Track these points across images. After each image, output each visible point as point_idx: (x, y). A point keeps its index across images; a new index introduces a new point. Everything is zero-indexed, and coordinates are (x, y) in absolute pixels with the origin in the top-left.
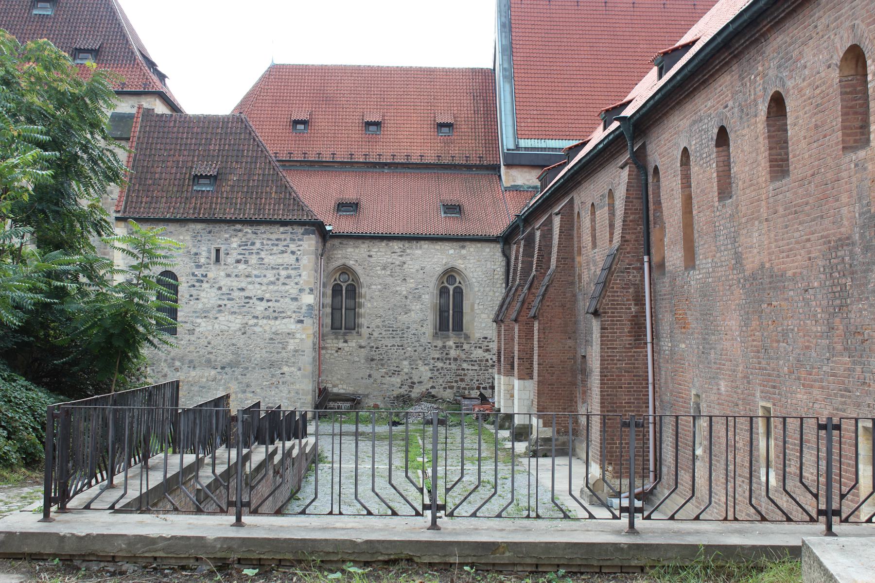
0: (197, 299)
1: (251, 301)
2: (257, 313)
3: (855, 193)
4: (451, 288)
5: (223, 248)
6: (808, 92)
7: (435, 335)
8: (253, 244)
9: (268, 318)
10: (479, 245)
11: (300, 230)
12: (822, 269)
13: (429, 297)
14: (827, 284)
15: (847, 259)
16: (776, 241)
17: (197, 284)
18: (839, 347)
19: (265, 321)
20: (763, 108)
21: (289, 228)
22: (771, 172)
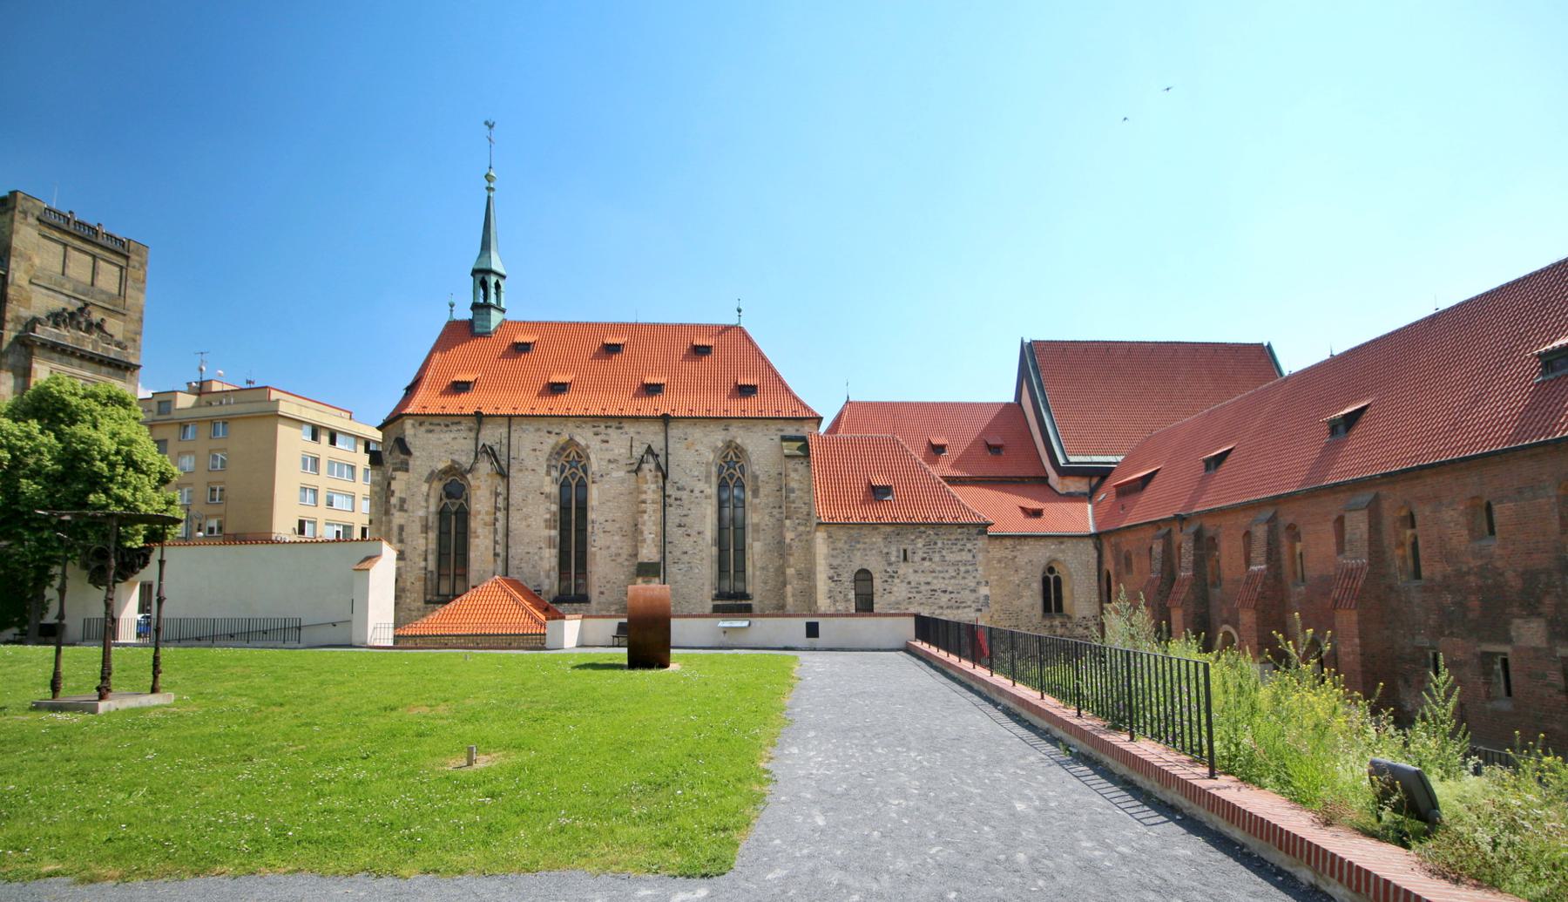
0: (890, 593)
1: (937, 594)
2: (942, 604)
4: (1052, 577)
5: (909, 548)
7: (1044, 617)
8: (935, 543)
9: (951, 607)
10: (1074, 541)
11: (974, 531)
13: (1037, 586)
17: (890, 580)
19: (949, 611)
21: (965, 530)
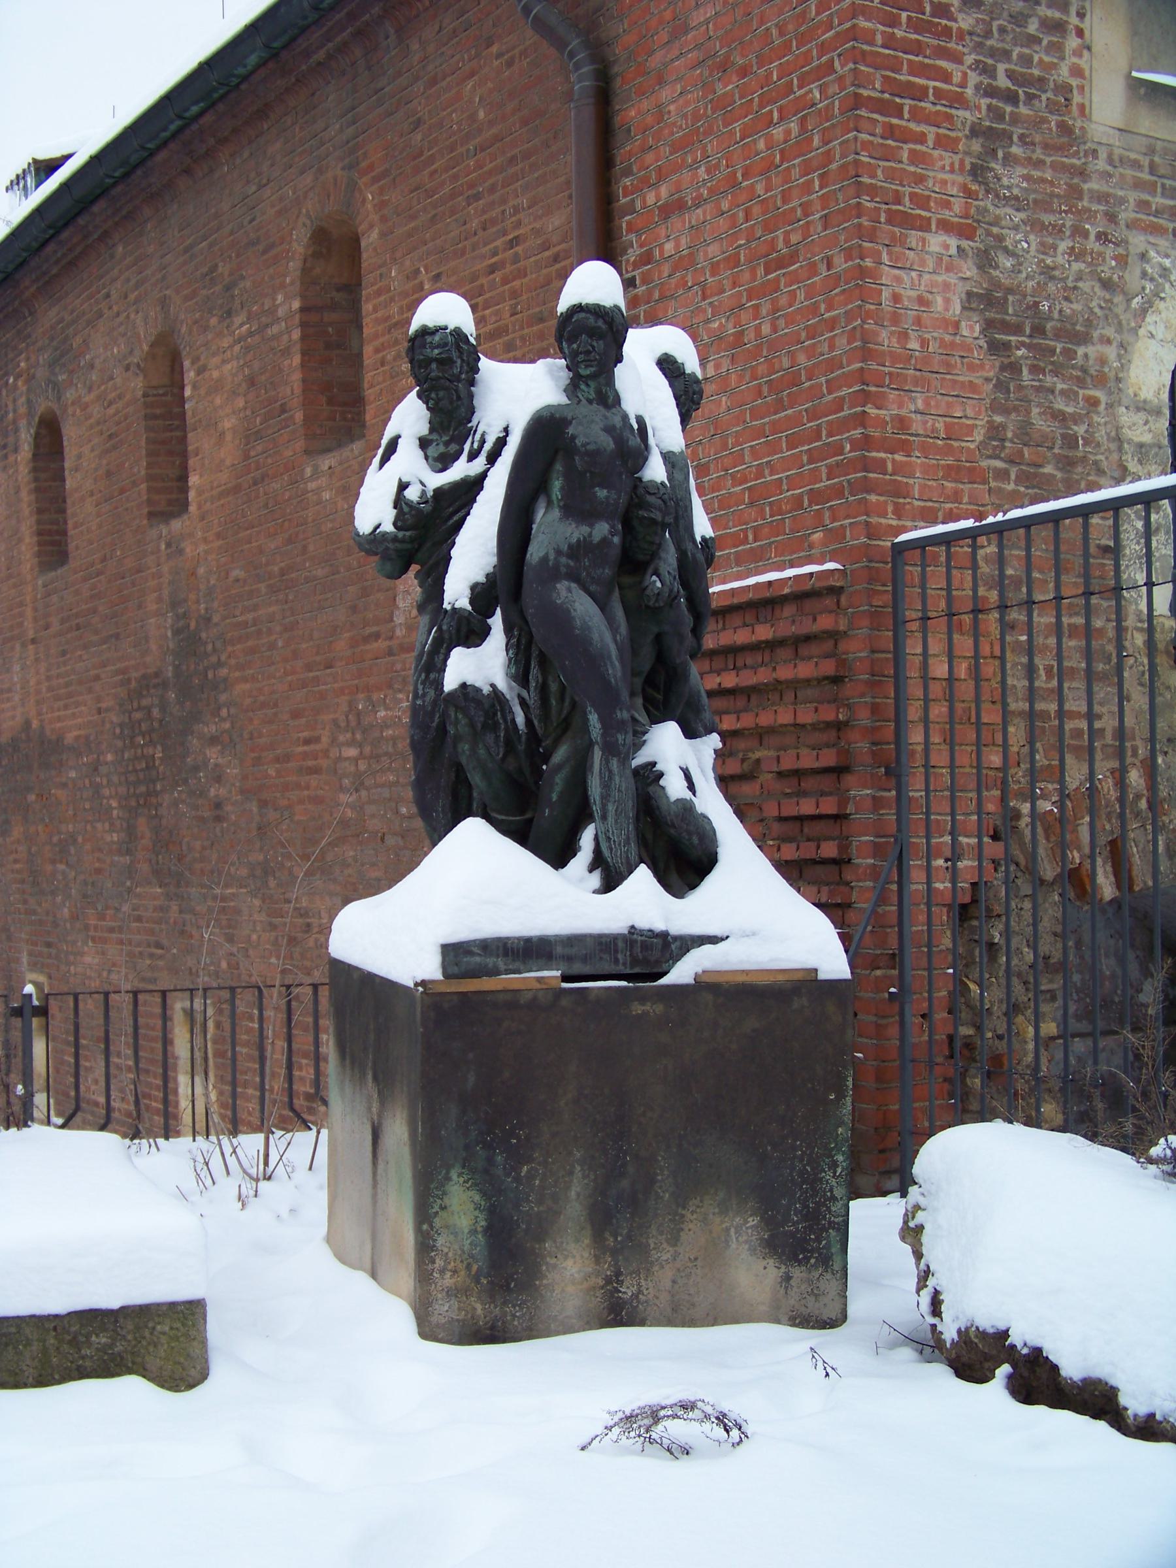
3: (166, 593)
6: (96, 411)
12: (118, 731)
14: (126, 756)
15: (156, 712)
16: (48, 678)
18: (144, 867)
20: (26, 438)
22: (39, 554)
